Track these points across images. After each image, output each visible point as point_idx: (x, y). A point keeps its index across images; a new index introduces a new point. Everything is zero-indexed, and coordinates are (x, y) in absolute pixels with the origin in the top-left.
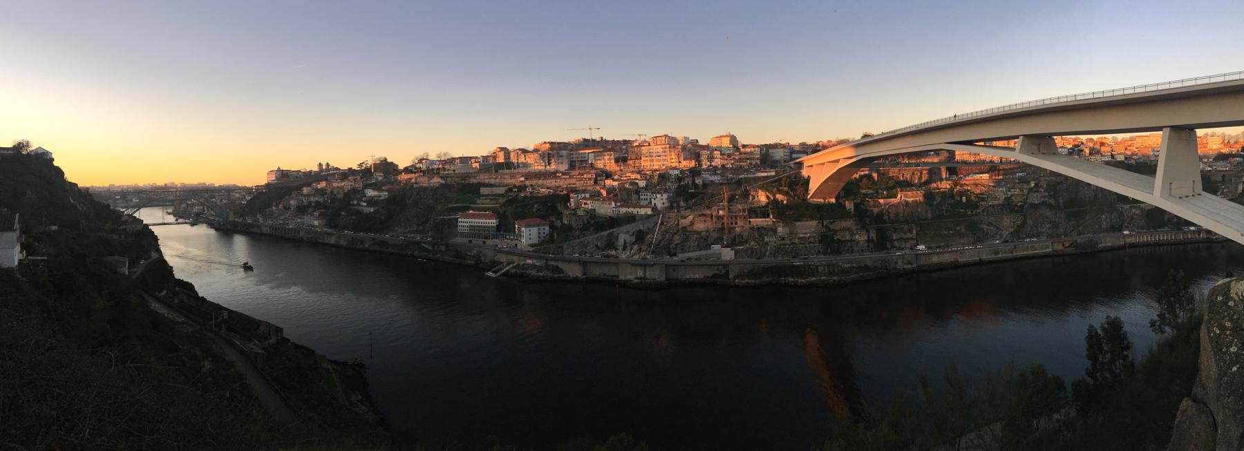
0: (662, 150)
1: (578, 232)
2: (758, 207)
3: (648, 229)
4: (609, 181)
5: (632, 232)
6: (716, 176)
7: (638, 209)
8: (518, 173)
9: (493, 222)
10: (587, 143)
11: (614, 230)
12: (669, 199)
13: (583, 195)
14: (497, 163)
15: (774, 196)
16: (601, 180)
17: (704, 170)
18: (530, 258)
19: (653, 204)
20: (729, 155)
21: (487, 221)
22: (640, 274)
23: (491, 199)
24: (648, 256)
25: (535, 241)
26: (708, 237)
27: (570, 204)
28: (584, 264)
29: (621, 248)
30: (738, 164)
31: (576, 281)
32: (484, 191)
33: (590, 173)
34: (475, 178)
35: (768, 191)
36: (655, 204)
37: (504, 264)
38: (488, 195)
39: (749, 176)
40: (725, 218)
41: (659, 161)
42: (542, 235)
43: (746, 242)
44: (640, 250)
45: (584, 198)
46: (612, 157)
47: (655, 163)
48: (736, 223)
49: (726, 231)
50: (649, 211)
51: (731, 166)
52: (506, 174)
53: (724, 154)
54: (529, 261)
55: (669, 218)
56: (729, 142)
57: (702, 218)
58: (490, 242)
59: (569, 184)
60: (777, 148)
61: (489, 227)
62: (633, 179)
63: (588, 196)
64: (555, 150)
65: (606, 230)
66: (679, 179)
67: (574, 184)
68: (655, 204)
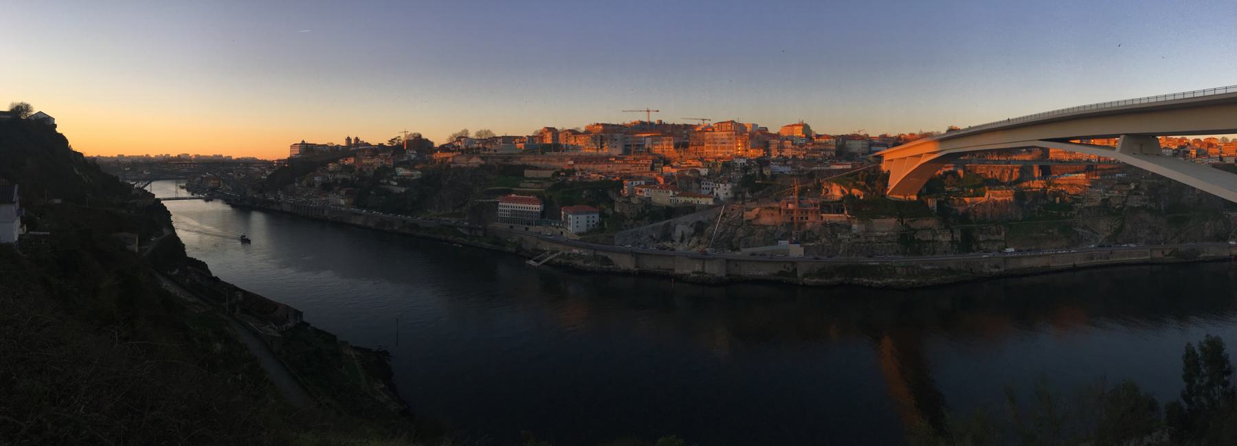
0: (727, 137)
1: (631, 222)
2: (832, 202)
3: (709, 220)
5: (691, 223)
6: (786, 167)
7: (698, 199)
8: (567, 156)
9: (537, 207)
10: (643, 126)
11: (671, 220)
12: (733, 189)
13: (638, 183)
14: (543, 144)
15: (850, 191)
16: (658, 167)
17: (773, 160)
18: (577, 247)
19: (715, 194)
20: (801, 146)
21: (531, 206)
22: (698, 267)
23: (535, 183)
24: (707, 250)
25: (584, 229)
26: (775, 231)
27: (624, 191)
28: (637, 255)
29: (678, 240)
30: (810, 155)
31: (626, 273)
32: (528, 173)
33: (646, 159)
34: (520, 160)
35: (843, 185)
36: (717, 195)
37: (548, 253)
38: (533, 178)
39: (823, 168)
40: (795, 212)
41: (722, 148)
42: (591, 224)
43: (817, 238)
44: (699, 242)
45: (640, 186)
46: (672, 142)
48: (807, 218)
49: (796, 226)
50: (711, 202)
51: (803, 157)
52: (554, 157)
53: (796, 144)
54: (576, 251)
55: (733, 210)
56: (801, 132)
57: (770, 211)
58: (532, 229)
59: (623, 170)
60: (855, 139)
61: (532, 212)
62: (694, 167)
63: (643, 183)
64: (607, 133)
65: (662, 220)
66: (745, 169)
67: (628, 170)
68: (717, 195)
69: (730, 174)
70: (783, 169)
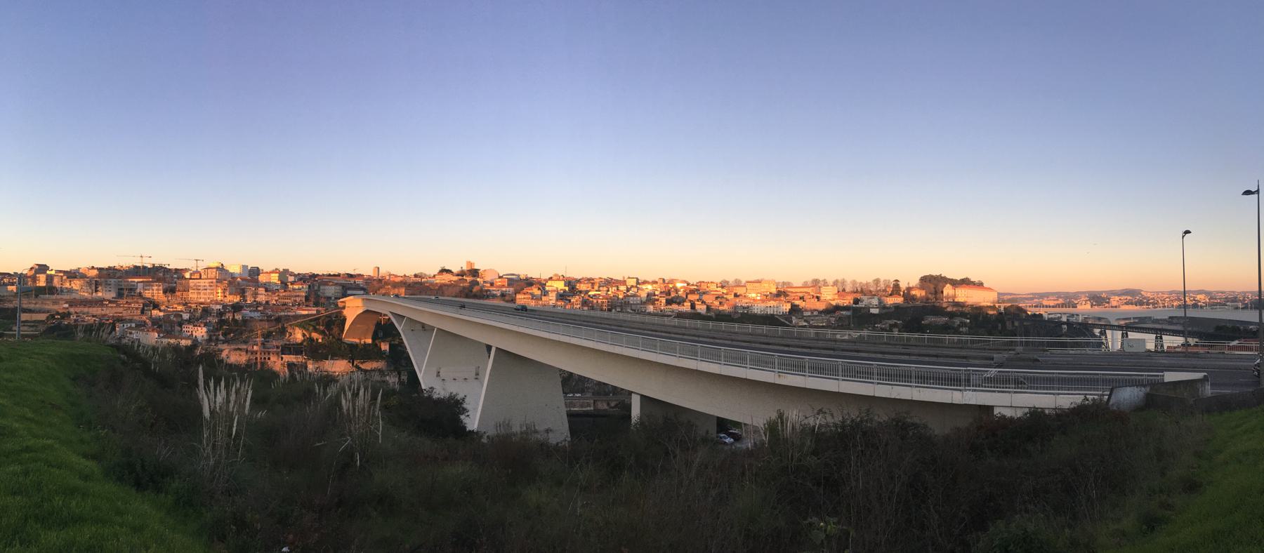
2: (294, 344)
4: (156, 311)
10: (137, 271)
13: (129, 325)
15: (310, 335)
33: (138, 303)
35: (305, 328)
36: (196, 337)
39: (289, 314)
40: (259, 353)
41: (205, 294)
47: (202, 296)
48: (269, 359)
57: (238, 352)
59: (116, 313)
62: (179, 311)
63: (133, 325)
64: (108, 275)
66: (220, 314)
67: (121, 313)
68: (196, 337)
69: (206, 319)
70: (253, 315)
